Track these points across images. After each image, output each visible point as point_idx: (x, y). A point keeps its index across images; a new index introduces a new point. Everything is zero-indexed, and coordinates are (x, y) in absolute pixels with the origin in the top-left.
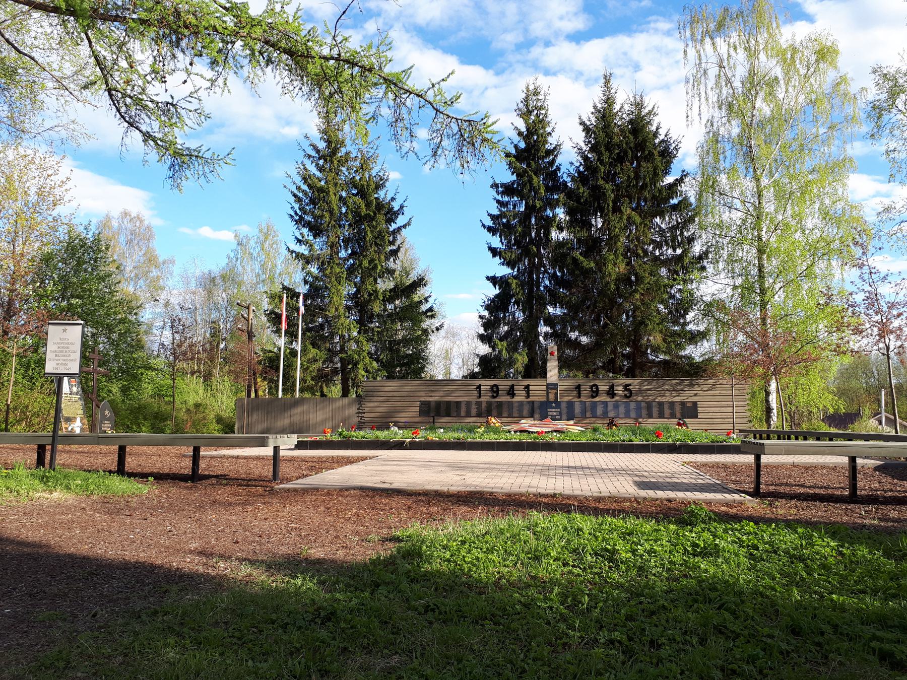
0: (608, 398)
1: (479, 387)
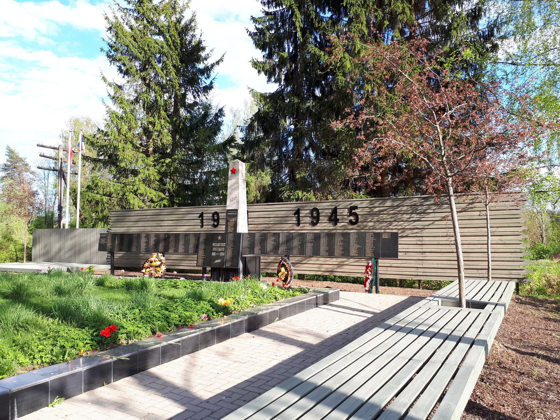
0: (331, 225)
1: (201, 215)
